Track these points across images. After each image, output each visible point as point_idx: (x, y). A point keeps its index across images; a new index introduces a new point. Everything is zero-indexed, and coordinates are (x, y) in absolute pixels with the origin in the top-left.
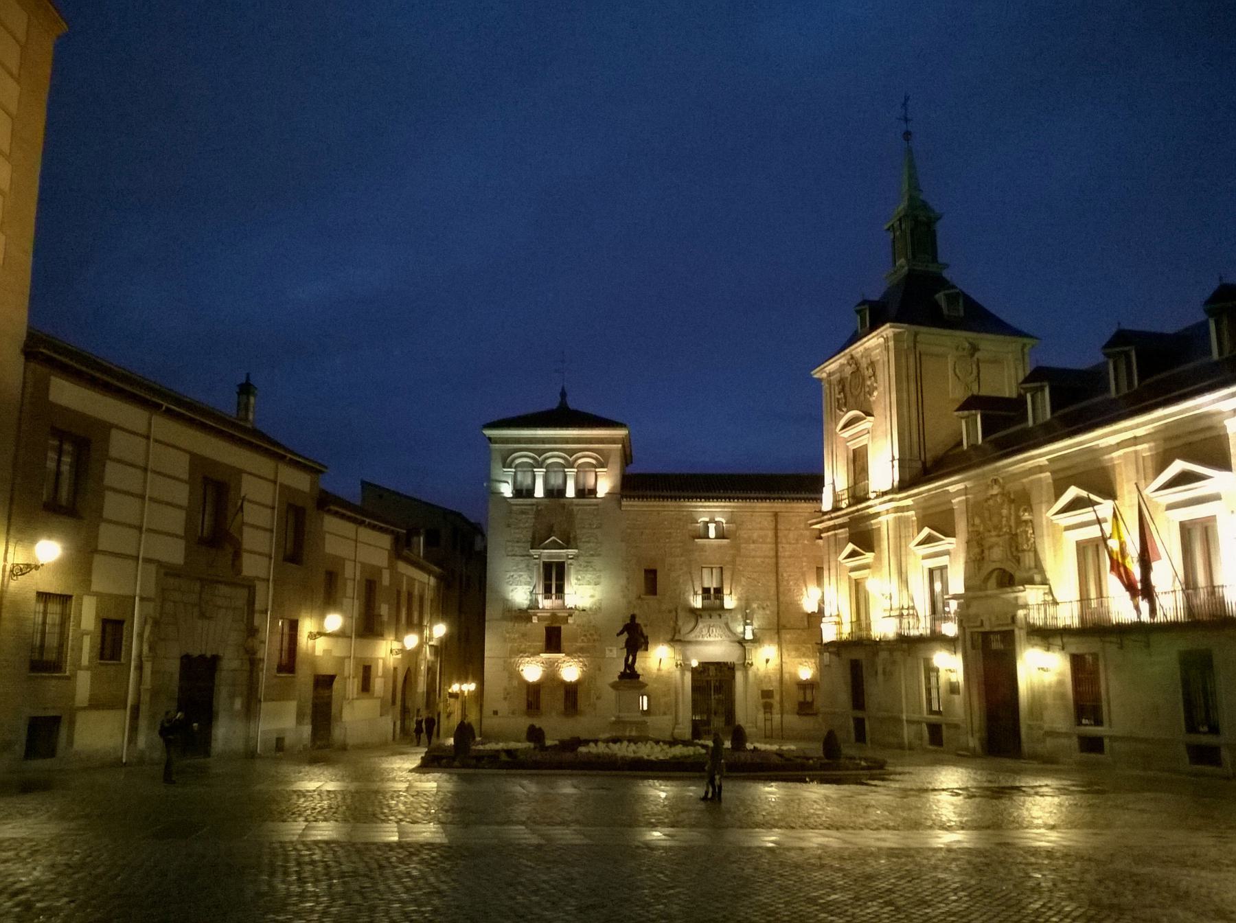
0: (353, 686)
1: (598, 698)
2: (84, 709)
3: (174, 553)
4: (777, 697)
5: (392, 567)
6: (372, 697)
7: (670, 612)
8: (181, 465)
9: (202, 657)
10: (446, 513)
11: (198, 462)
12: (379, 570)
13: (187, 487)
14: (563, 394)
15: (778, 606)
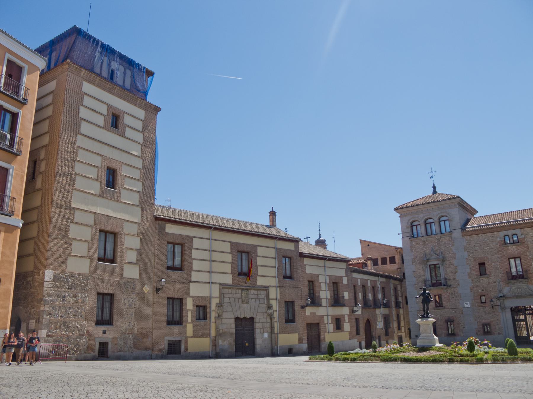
0: (331, 327)
1: (464, 327)
2: (191, 337)
3: (228, 279)
5: (347, 276)
6: (343, 331)
7: (495, 282)
8: (227, 247)
9: (245, 318)
10: (397, 248)
11: (233, 244)
12: (341, 278)
13: (230, 255)
14: (434, 187)
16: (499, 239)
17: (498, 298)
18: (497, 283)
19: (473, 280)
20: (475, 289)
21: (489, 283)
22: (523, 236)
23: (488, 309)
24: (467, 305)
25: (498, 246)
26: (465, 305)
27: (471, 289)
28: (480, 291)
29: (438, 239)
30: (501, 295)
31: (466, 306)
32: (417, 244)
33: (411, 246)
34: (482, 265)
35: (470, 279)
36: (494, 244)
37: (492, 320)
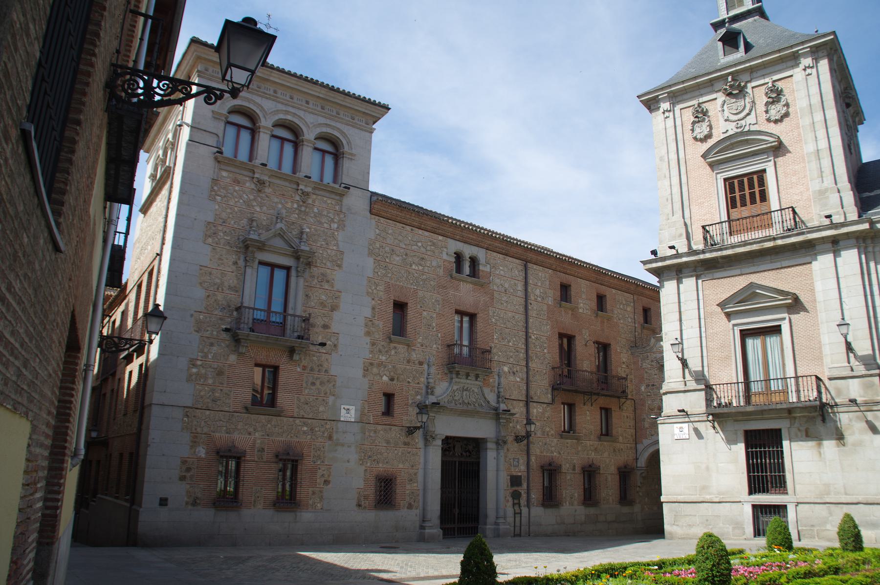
1: (326, 482)
4: (525, 486)
7: (421, 363)
15: (527, 373)
16: (445, 257)
17: (423, 408)
18: (425, 366)
19: (373, 344)
20: (375, 370)
21: (408, 362)
22: (487, 269)
23: (396, 434)
24: (349, 413)
25: (441, 272)
26: (343, 412)
27: (366, 370)
28: (385, 378)
29: (305, 194)
30: (432, 399)
31: (344, 416)
32: (237, 182)
33: (215, 181)
34: (400, 307)
35: (368, 339)
36: (434, 264)
37: (401, 466)
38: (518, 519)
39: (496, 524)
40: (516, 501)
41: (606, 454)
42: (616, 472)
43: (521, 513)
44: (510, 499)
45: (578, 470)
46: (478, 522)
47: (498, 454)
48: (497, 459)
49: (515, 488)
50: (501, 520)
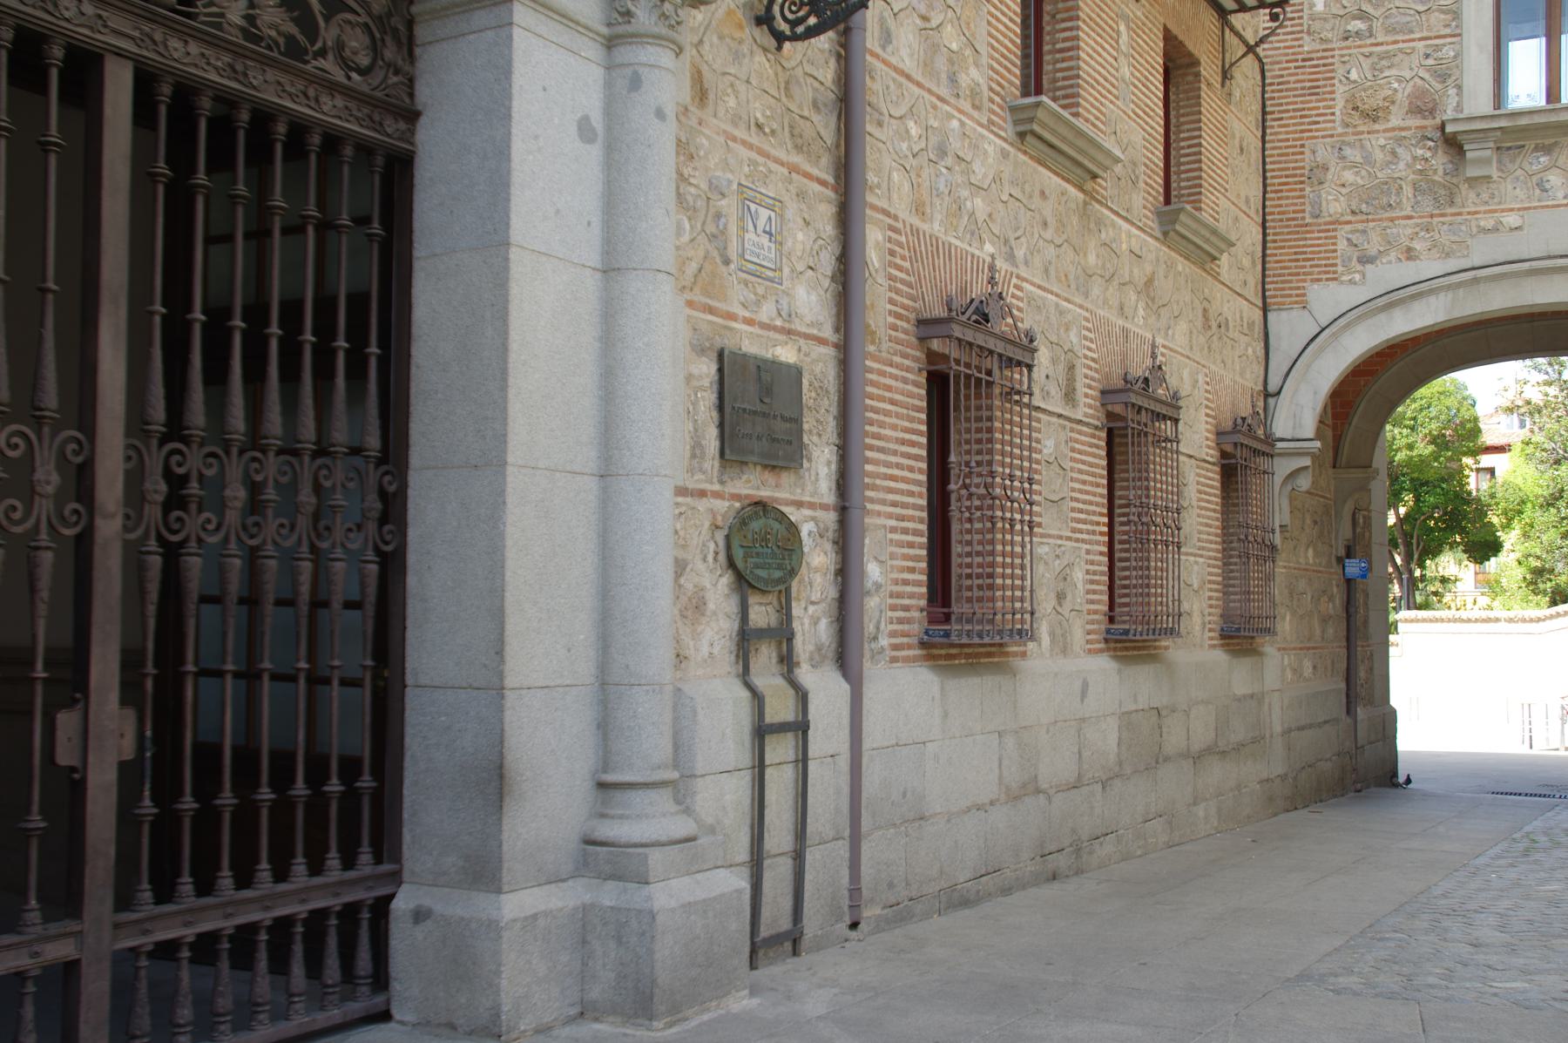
38: (780, 783)
39: (600, 857)
40: (762, 614)
41: (1183, 326)
42: (1212, 454)
43: (801, 728)
44: (718, 589)
45: (1087, 407)
46: (386, 844)
47: (622, 84)
48: (612, 139)
49: (753, 484)
50: (647, 821)
